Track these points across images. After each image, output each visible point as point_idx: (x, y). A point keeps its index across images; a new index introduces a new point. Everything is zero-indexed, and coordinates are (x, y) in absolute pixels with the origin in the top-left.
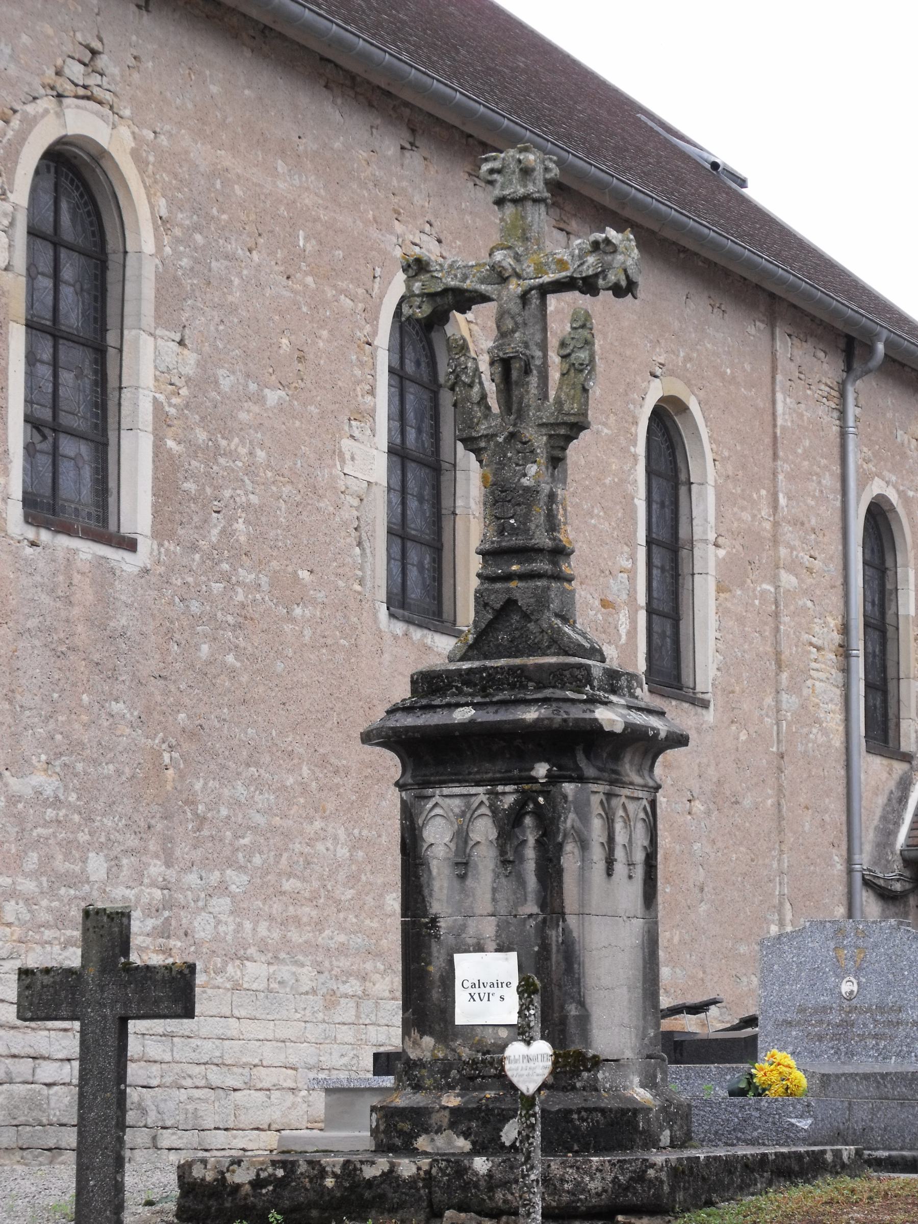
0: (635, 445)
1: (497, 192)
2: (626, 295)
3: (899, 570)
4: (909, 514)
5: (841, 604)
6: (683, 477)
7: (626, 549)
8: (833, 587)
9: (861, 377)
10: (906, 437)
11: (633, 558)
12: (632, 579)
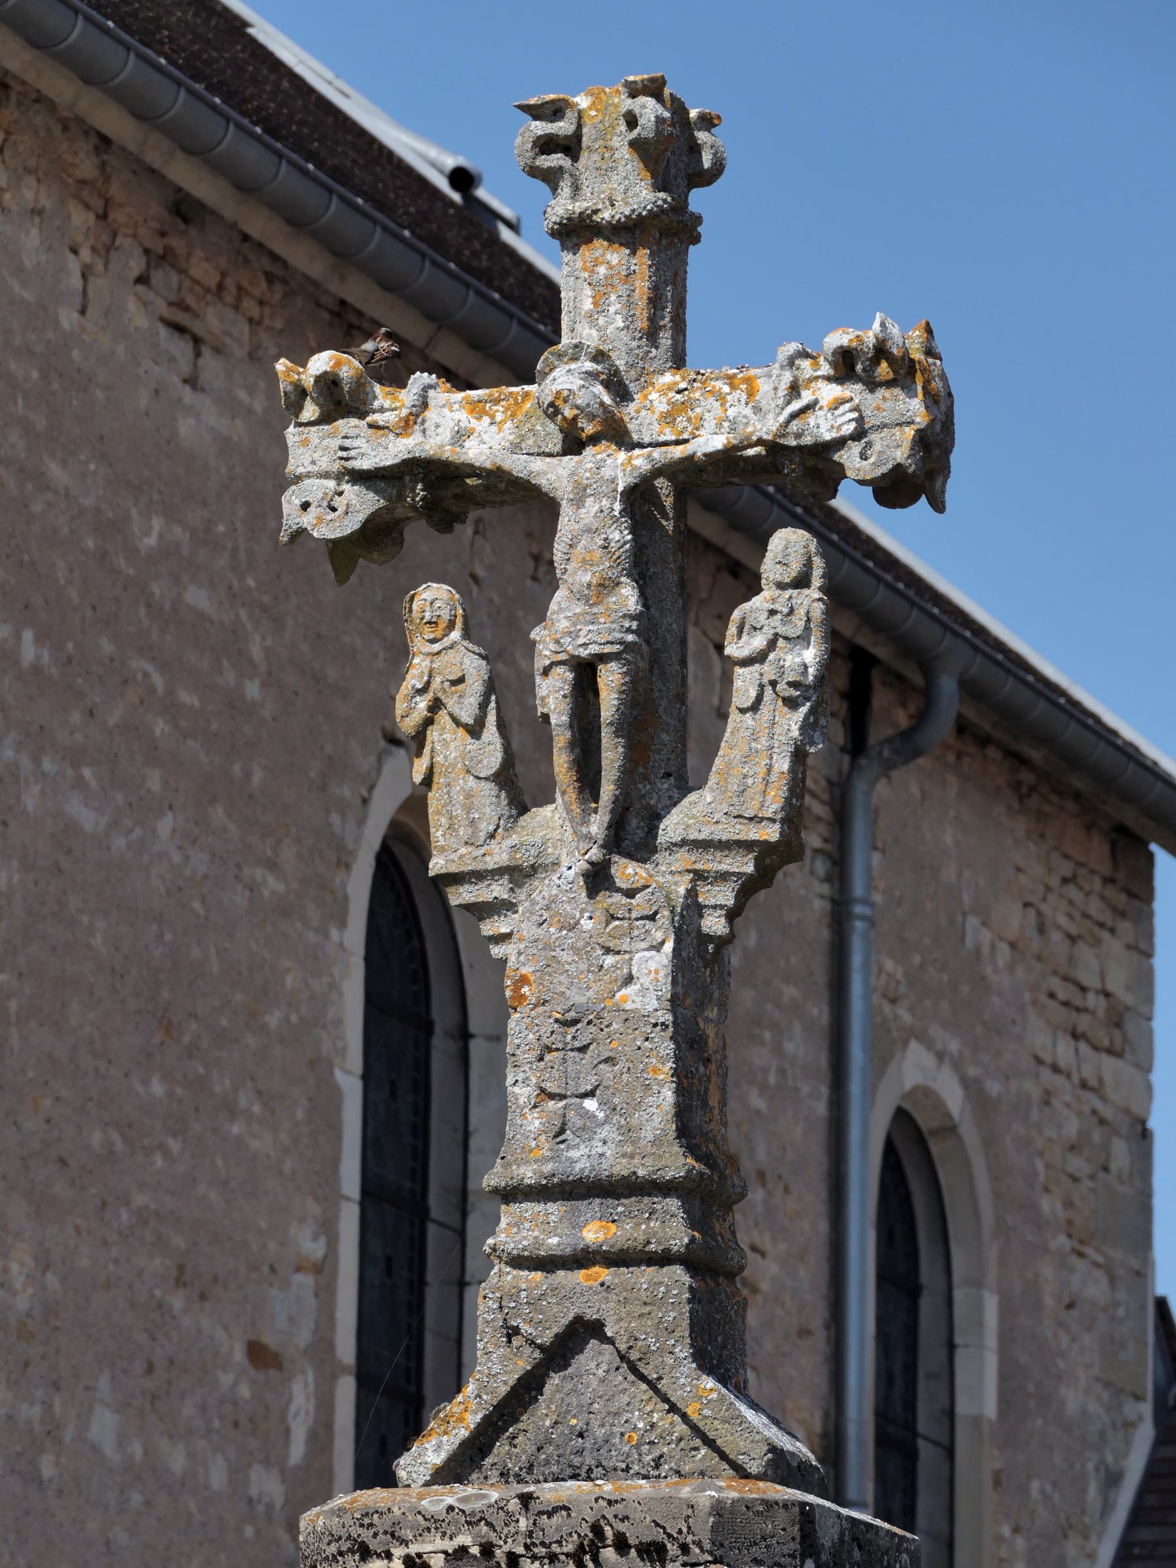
0: (343, 924)
1: (562, 206)
2: (913, 500)
3: (959, 1294)
4: (990, 1142)
5: (821, 1380)
6: (442, 1015)
7: (314, 1209)
8: (805, 1332)
9: (888, 767)
10: (986, 936)
11: (328, 1228)
12: (326, 1295)
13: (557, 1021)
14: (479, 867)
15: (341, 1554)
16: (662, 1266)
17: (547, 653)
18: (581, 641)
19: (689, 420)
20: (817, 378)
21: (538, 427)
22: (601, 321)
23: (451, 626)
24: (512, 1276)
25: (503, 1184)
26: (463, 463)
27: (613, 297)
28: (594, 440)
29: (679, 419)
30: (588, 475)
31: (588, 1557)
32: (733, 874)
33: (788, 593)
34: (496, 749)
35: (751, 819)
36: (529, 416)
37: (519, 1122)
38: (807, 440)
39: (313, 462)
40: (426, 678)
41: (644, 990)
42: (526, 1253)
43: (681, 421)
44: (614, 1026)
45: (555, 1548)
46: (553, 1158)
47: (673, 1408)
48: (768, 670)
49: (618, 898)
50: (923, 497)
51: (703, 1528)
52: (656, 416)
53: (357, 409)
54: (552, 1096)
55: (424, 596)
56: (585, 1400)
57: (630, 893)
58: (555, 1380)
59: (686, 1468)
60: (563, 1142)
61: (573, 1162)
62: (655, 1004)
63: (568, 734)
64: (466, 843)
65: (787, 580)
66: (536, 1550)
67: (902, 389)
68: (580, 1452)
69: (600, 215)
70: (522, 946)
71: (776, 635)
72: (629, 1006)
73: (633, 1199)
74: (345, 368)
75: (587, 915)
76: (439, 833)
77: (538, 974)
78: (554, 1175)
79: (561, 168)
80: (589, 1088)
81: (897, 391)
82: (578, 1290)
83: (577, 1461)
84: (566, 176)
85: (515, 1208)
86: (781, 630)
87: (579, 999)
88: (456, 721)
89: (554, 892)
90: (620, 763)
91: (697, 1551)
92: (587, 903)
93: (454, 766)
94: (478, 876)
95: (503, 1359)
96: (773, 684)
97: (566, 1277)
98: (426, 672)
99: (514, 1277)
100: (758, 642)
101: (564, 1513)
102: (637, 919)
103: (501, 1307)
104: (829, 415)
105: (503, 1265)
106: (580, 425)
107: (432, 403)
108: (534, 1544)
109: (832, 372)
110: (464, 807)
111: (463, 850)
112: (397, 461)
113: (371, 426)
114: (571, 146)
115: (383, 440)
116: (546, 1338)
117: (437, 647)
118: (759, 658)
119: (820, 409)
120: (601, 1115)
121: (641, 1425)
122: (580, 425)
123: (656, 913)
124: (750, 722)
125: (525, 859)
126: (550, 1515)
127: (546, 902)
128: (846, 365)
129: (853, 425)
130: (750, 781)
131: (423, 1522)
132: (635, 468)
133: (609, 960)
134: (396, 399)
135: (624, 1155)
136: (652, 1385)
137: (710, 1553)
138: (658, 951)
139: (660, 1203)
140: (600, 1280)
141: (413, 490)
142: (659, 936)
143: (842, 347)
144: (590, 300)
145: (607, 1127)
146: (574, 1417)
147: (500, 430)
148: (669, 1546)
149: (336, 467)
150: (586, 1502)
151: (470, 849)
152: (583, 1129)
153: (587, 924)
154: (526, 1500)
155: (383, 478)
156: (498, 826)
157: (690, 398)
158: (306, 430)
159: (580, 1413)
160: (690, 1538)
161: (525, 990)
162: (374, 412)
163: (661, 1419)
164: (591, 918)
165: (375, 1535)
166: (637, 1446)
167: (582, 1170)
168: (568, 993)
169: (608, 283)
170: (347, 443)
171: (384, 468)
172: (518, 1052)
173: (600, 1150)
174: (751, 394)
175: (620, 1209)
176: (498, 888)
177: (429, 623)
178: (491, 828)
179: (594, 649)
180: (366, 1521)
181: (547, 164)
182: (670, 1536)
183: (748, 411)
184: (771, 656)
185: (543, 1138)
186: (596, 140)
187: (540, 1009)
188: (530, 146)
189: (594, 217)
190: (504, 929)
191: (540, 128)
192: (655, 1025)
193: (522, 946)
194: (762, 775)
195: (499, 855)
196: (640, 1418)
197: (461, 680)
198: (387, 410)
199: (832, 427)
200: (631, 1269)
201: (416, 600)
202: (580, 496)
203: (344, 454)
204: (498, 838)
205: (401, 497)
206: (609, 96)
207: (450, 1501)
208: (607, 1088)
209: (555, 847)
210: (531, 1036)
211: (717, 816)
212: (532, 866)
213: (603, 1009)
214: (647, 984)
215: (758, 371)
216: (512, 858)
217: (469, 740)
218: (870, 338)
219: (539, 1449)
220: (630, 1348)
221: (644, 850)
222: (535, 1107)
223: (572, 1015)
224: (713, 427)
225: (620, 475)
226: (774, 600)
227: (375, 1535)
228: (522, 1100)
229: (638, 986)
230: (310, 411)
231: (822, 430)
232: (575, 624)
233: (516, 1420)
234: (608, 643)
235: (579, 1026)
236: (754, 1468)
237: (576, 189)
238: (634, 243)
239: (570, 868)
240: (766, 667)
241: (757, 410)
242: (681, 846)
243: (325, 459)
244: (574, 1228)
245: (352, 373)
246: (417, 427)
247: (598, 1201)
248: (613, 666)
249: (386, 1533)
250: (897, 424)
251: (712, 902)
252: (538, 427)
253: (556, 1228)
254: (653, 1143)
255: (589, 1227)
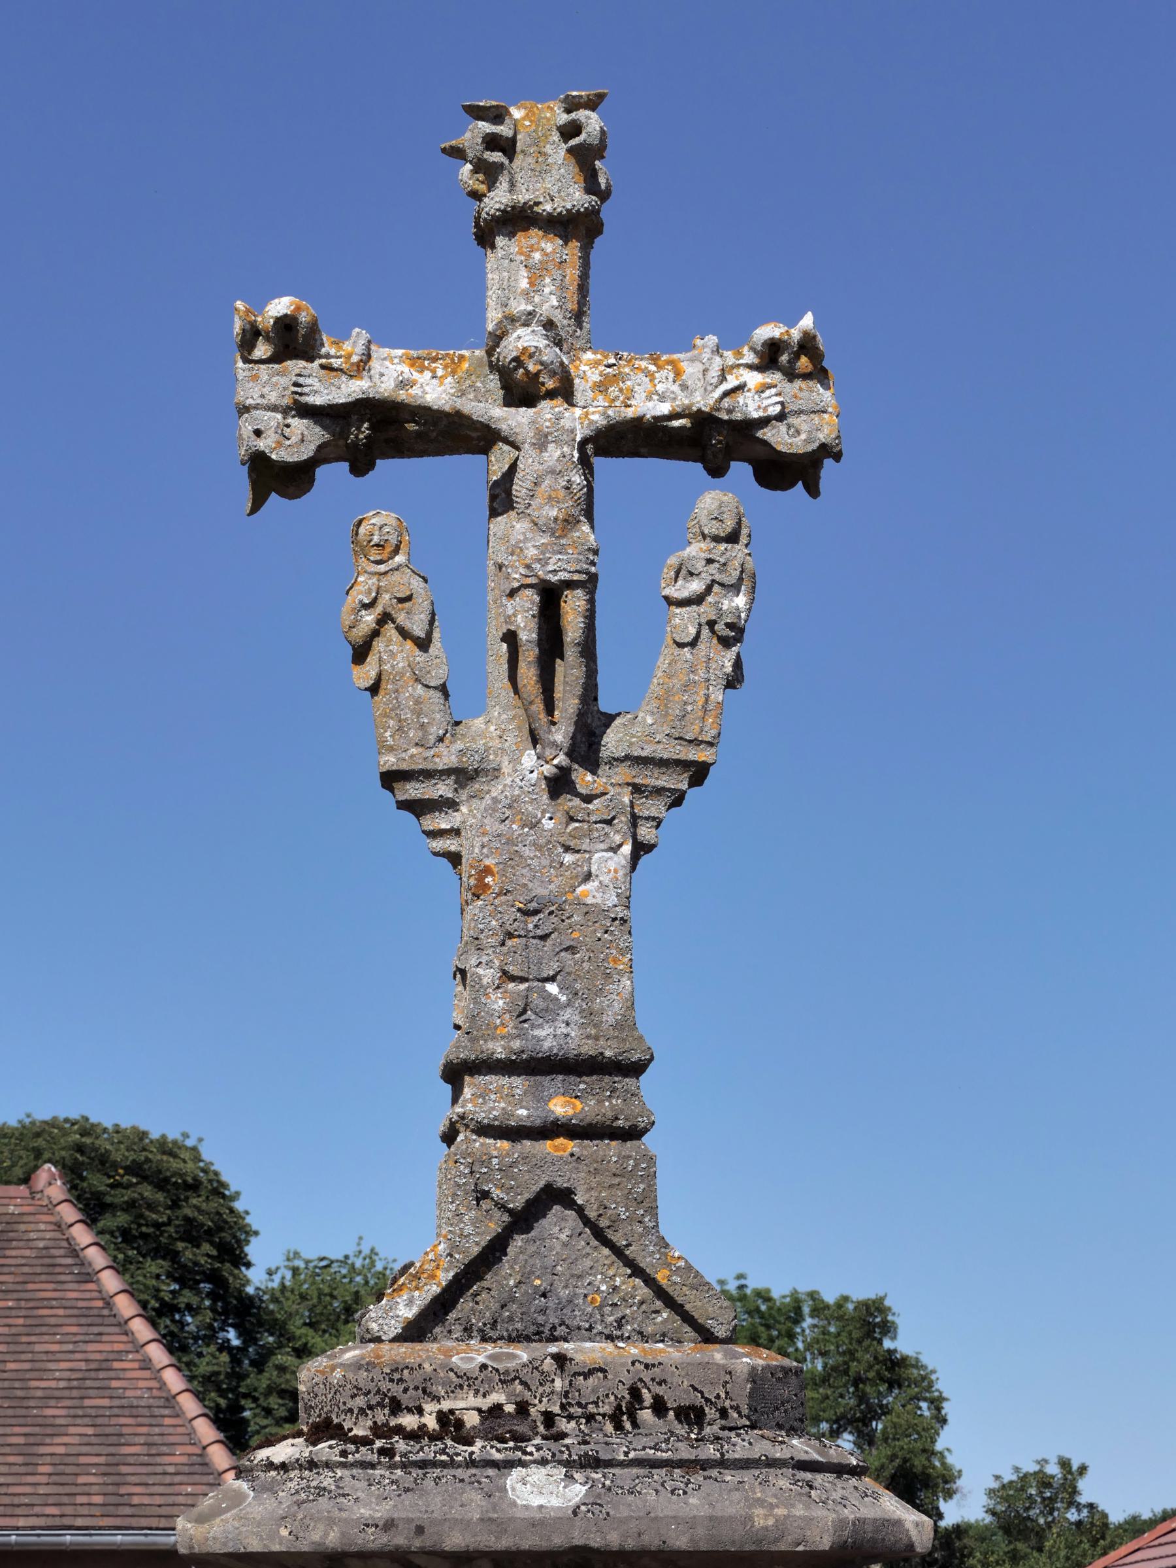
2: (792, 485)
13: (519, 910)
14: (430, 766)
15: (371, 1408)
16: (625, 1140)
17: (517, 576)
18: (551, 568)
19: (621, 390)
20: (739, 366)
21: (479, 384)
22: (537, 299)
23: (396, 551)
24: (479, 1142)
25: (473, 1057)
26: (419, 407)
27: (547, 280)
28: (551, 395)
29: (611, 389)
30: (548, 424)
31: (625, 1418)
32: (669, 790)
33: (723, 546)
34: (442, 663)
35: (690, 741)
36: (469, 373)
37: (483, 1000)
38: (738, 416)
39: (262, 396)
40: (374, 594)
41: (603, 886)
42: (496, 1123)
43: (613, 391)
44: (575, 917)
45: (591, 1408)
46: (519, 1035)
47: (637, 1271)
48: (706, 611)
49: (577, 802)
50: (800, 483)
51: (742, 1394)
52: (590, 384)
53: (306, 353)
54: (513, 978)
55: (373, 521)
56: (549, 1262)
57: (588, 799)
58: (518, 1241)
59: (649, 1330)
60: (525, 1021)
61: (539, 1040)
62: (615, 900)
63: (537, 650)
64: (417, 744)
65: (723, 535)
66: (572, 1410)
67: (819, 382)
68: (543, 1311)
69: (541, 207)
70: (486, 839)
71: (713, 581)
72: (590, 901)
73: (594, 1077)
74: (304, 314)
75: (548, 815)
76: (388, 734)
77: (501, 866)
78: (523, 1052)
79: (502, 164)
80: (551, 973)
81: (811, 383)
82: (549, 1159)
83: (541, 1319)
84: (506, 172)
85: (481, 1080)
86: (718, 577)
87: (542, 892)
88: (404, 633)
89: (516, 793)
90: (583, 680)
91: (736, 1415)
92: (548, 805)
93: (402, 675)
94: (427, 775)
95: (474, 1222)
96: (711, 624)
97: (534, 1147)
98: (374, 588)
99: (482, 1145)
100: (695, 586)
101: (601, 1375)
102: (596, 823)
103: (472, 1172)
104: (756, 397)
105: (468, 1133)
106: (541, 379)
107: (374, 355)
108: (570, 1404)
109: (756, 361)
110: (413, 712)
111: (414, 751)
112: (350, 400)
113: (323, 367)
114: (507, 146)
115: (335, 381)
116: (518, 1203)
117: (382, 568)
118: (697, 600)
119: (749, 390)
120: (563, 998)
121: (604, 1288)
122: (541, 379)
123: (614, 818)
124: (689, 656)
125: (471, 763)
126: (586, 1375)
127: (508, 801)
128: (771, 356)
129: (778, 408)
130: (689, 708)
131: (455, 1379)
132: (592, 422)
133: (568, 858)
134: (340, 348)
135: (588, 1037)
136: (618, 1252)
137: (748, 1418)
138: (615, 853)
139: (619, 1082)
140: (569, 1151)
141: (359, 429)
142: (618, 839)
143: (772, 339)
144: (526, 280)
145: (569, 1010)
146: (538, 1277)
147: (441, 384)
148: (707, 1410)
149: (286, 401)
150: (623, 1365)
151: (420, 750)
152: (547, 1010)
153: (548, 824)
154: (561, 1360)
155: (328, 415)
156: (447, 732)
157: (620, 373)
158: (256, 367)
159: (544, 1274)
160: (727, 1403)
161: (489, 880)
162: (321, 357)
163: (623, 1283)
164: (551, 819)
165: (406, 1390)
166: (600, 1308)
167: (551, 1049)
168: (530, 885)
169: (544, 267)
170: (301, 380)
171: (337, 405)
172: (481, 936)
173: (565, 1031)
174: (678, 373)
175: (582, 1086)
176: (443, 788)
177: (377, 545)
178: (441, 732)
179: (563, 576)
180: (396, 1376)
181: (491, 160)
182: (707, 1400)
183: (675, 388)
184: (710, 599)
185: (507, 1016)
186: (530, 146)
187: (503, 898)
188: (480, 140)
189: (535, 209)
190: (444, 826)
191: (485, 127)
192: (614, 919)
193: (486, 839)
194: (700, 703)
195: (447, 757)
196: (603, 1281)
197: (409, 598)
198: (333, 357)
199: (759, 407)
200: (595, 1142)
201: (364, 524)
202: (541, 443)
203: (296, 389)
204: (447, 742)
205: (344, 434)
206: (541, 111)
207: (481, 1359)
208: (569, 974)
209: (496, 755)
210: (494, 922)
211: (658, 737)
212: (476, 770)
213: (565, 902)
214: (607, 882)
215: (682, 356)
216: (460, 761)
217: (418, 652)
218: (796, 334)
219: (503, 1306)
220: (600, 1215)
221: (593, 765)
222: (498, 987)
223: (533, 906)
224: (644, 398)
225: (579, 427)
226: (710, 551)
227: (406, 1390)
228: (485, 981)
229: (596, 883)
230: (262, 350)
231: (751, 408)
232: (543, 553)
233: (481, 1279)
234: (577, 571)
235: (542, 915)
236: (721, 1332)
237: (512, 185)
238: (566, 237)
239: (532, 772)
240: (702, 609)
241: (684, 387)
242: (622, 761)
243: (274, 394)
244: (538, 1101)
245: (309, 319)
246: (365, 373)
247: (560, 1077)
248: (579, 592)
249: (416, 1388)
250: (813, 412)
251: (647, 813)
252: (479, 384)
253: (521, 1101)
254: (614, 1027)
255: (554, 1101)
